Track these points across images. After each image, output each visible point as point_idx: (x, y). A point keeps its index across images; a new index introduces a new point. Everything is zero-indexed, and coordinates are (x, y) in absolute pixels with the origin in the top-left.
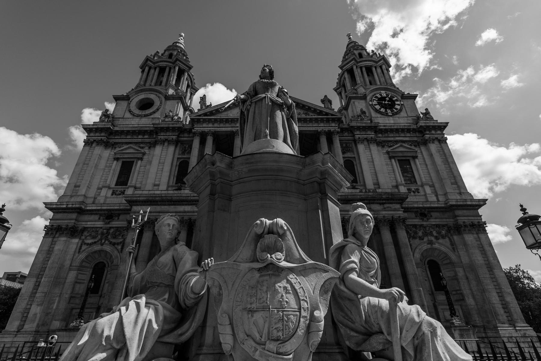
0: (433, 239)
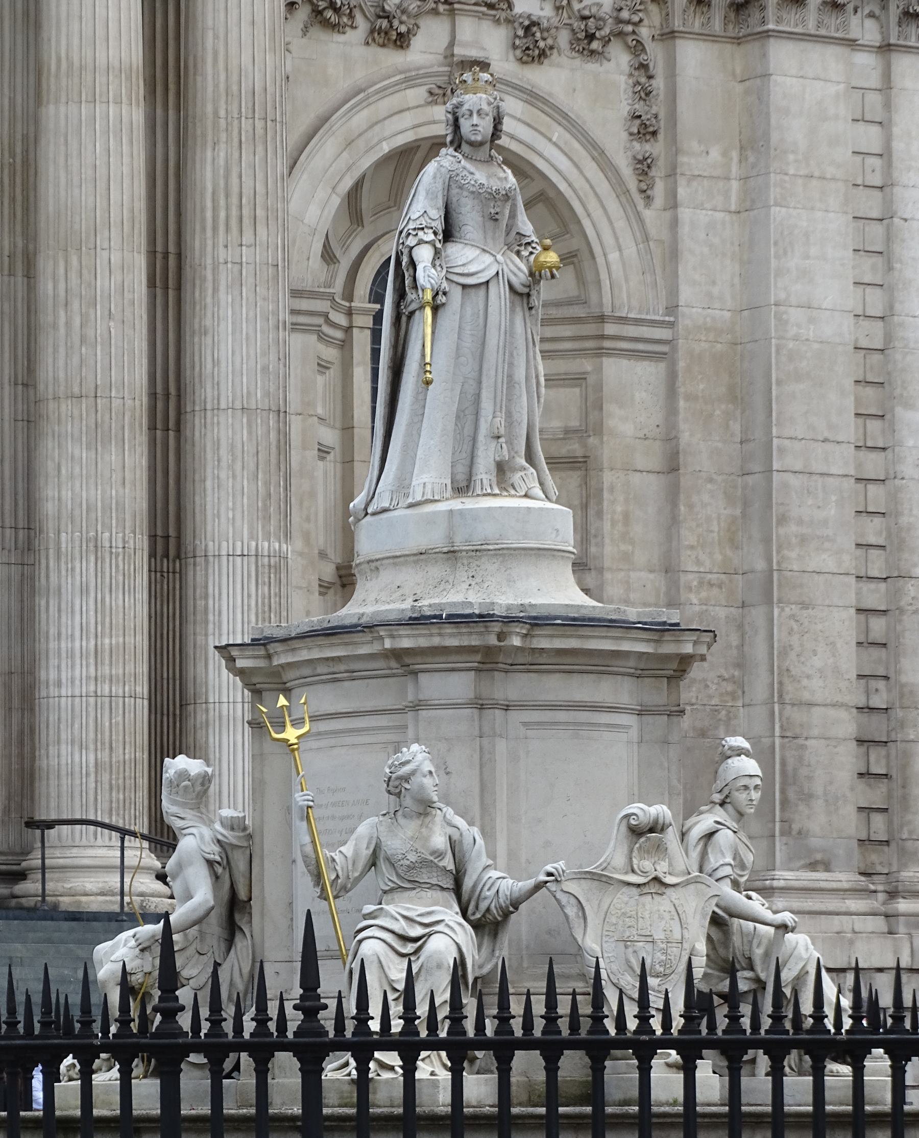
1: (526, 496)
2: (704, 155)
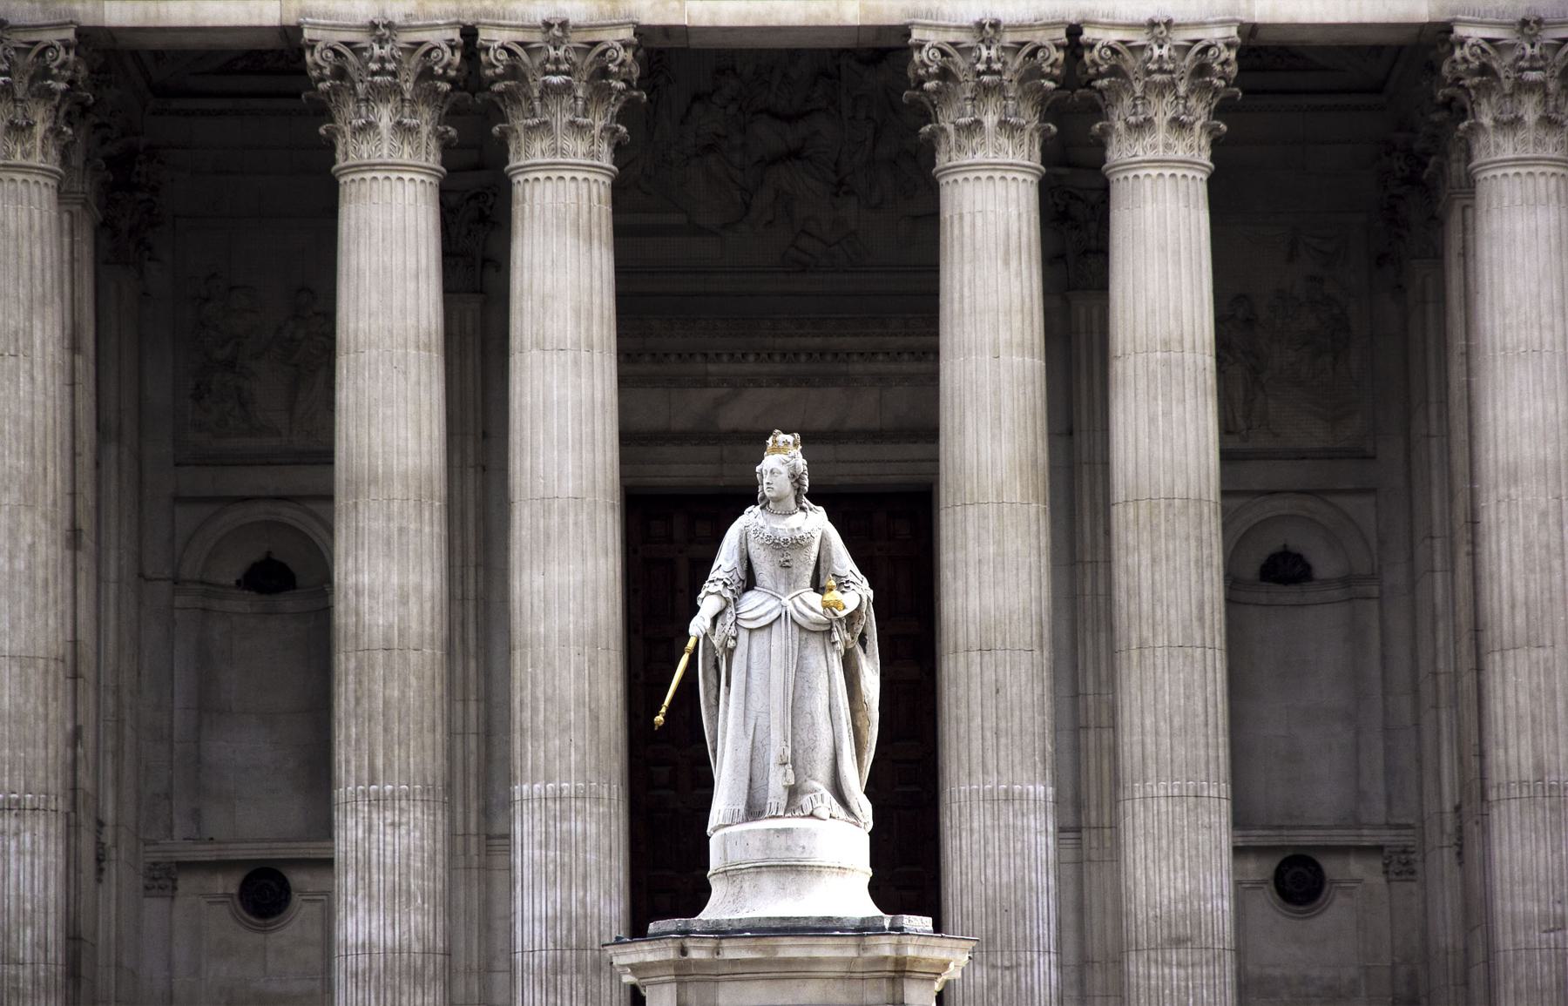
1: (812, 815)
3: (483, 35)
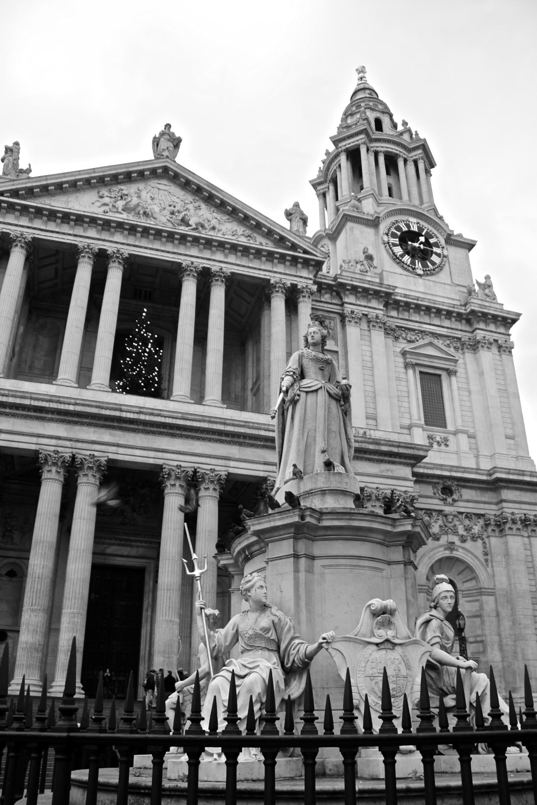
0: (456, 539)
2: (498, 558)
3: (77, 455)
